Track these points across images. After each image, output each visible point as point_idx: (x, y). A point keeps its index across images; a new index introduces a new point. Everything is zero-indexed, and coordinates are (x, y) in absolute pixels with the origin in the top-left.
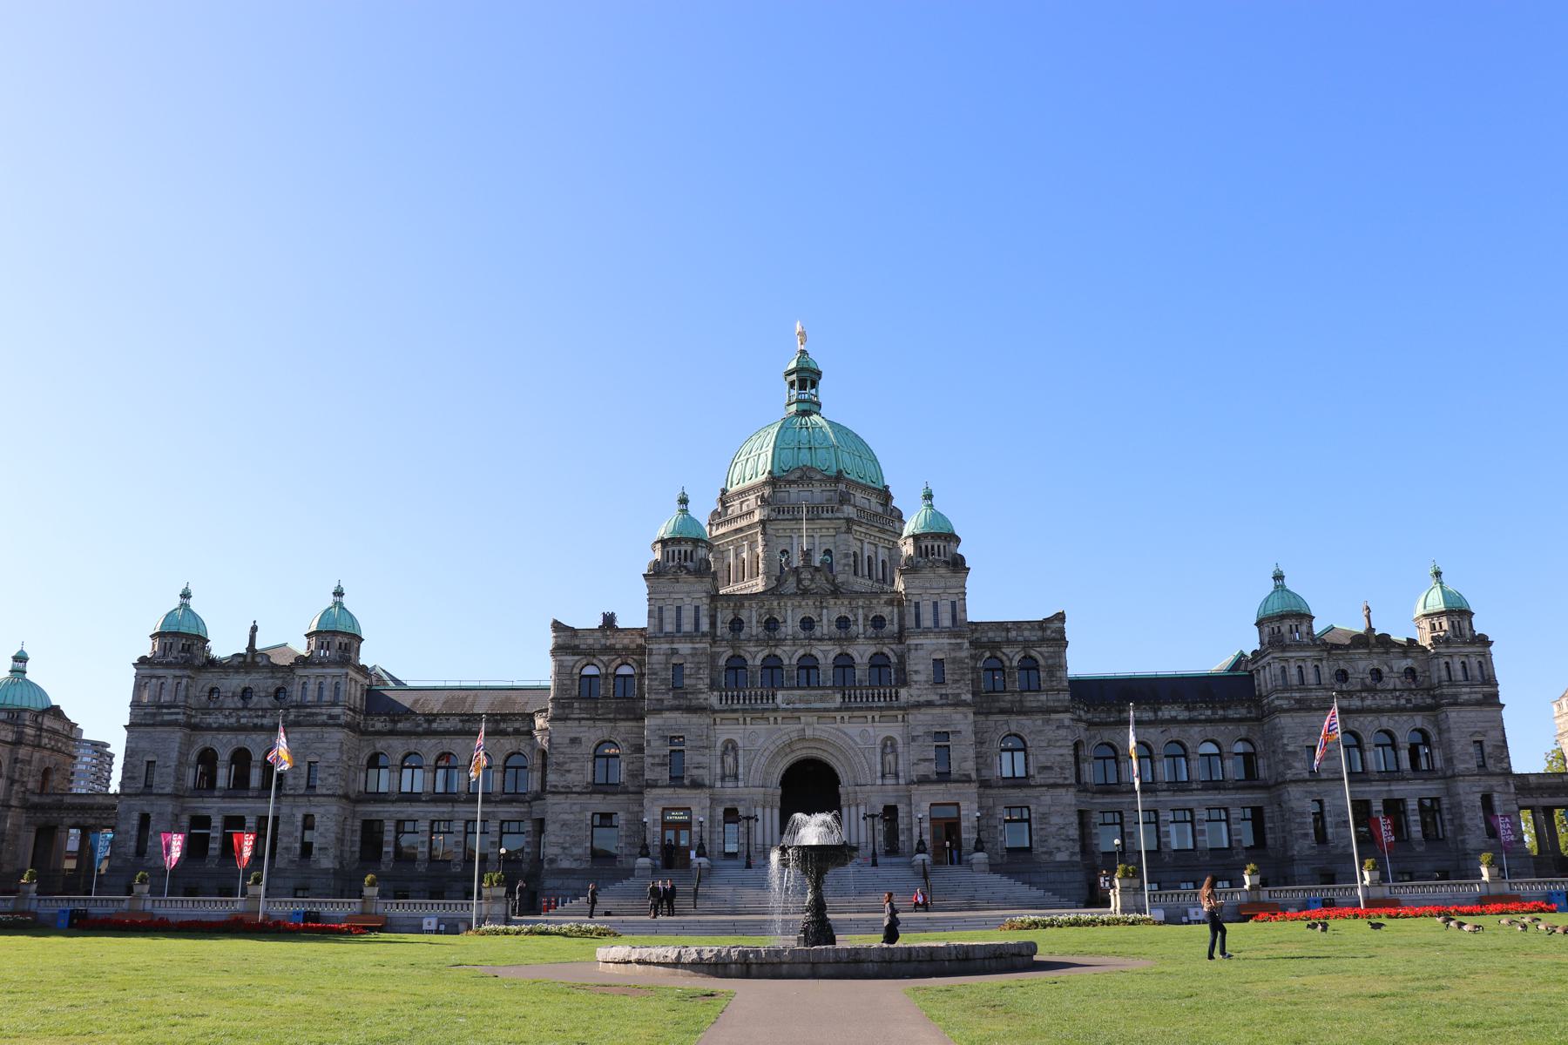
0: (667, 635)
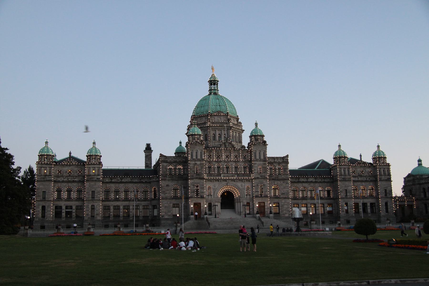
0: (194, 159)
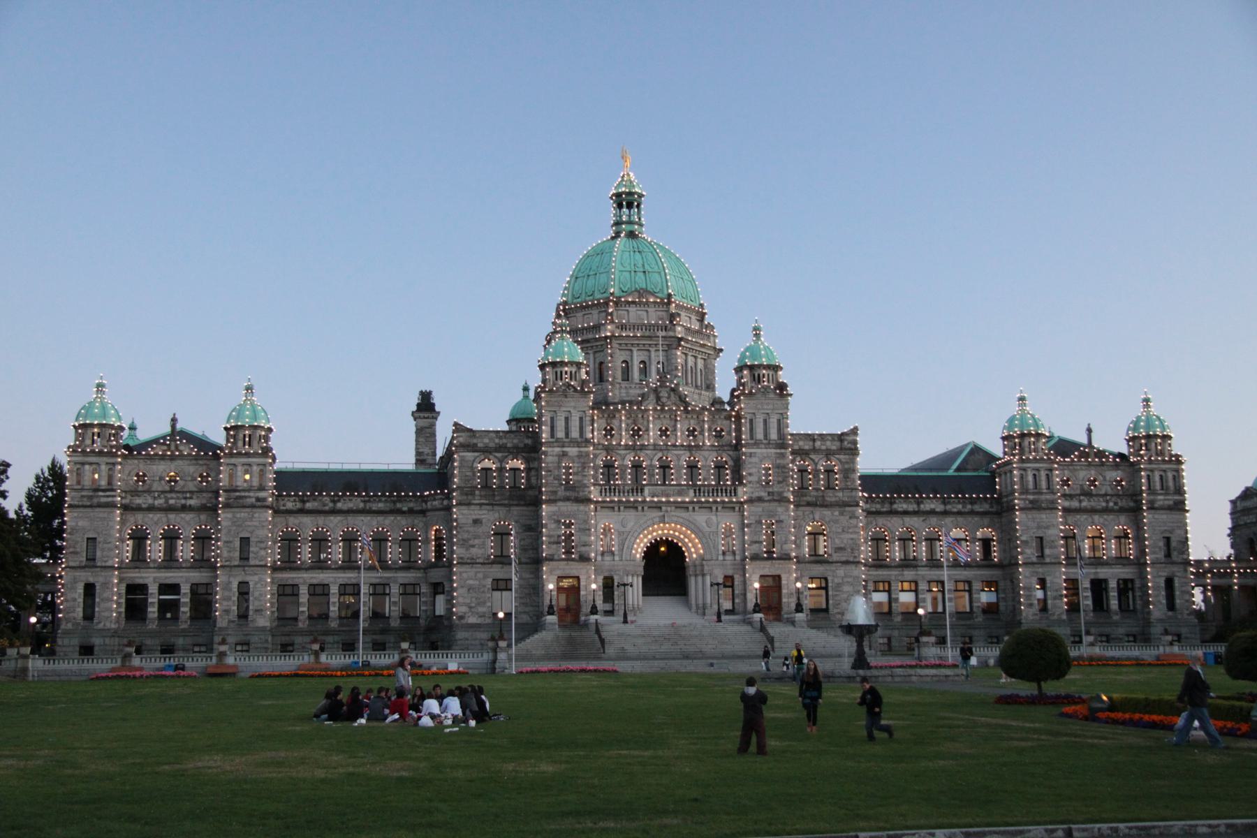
0: (558, 440)
